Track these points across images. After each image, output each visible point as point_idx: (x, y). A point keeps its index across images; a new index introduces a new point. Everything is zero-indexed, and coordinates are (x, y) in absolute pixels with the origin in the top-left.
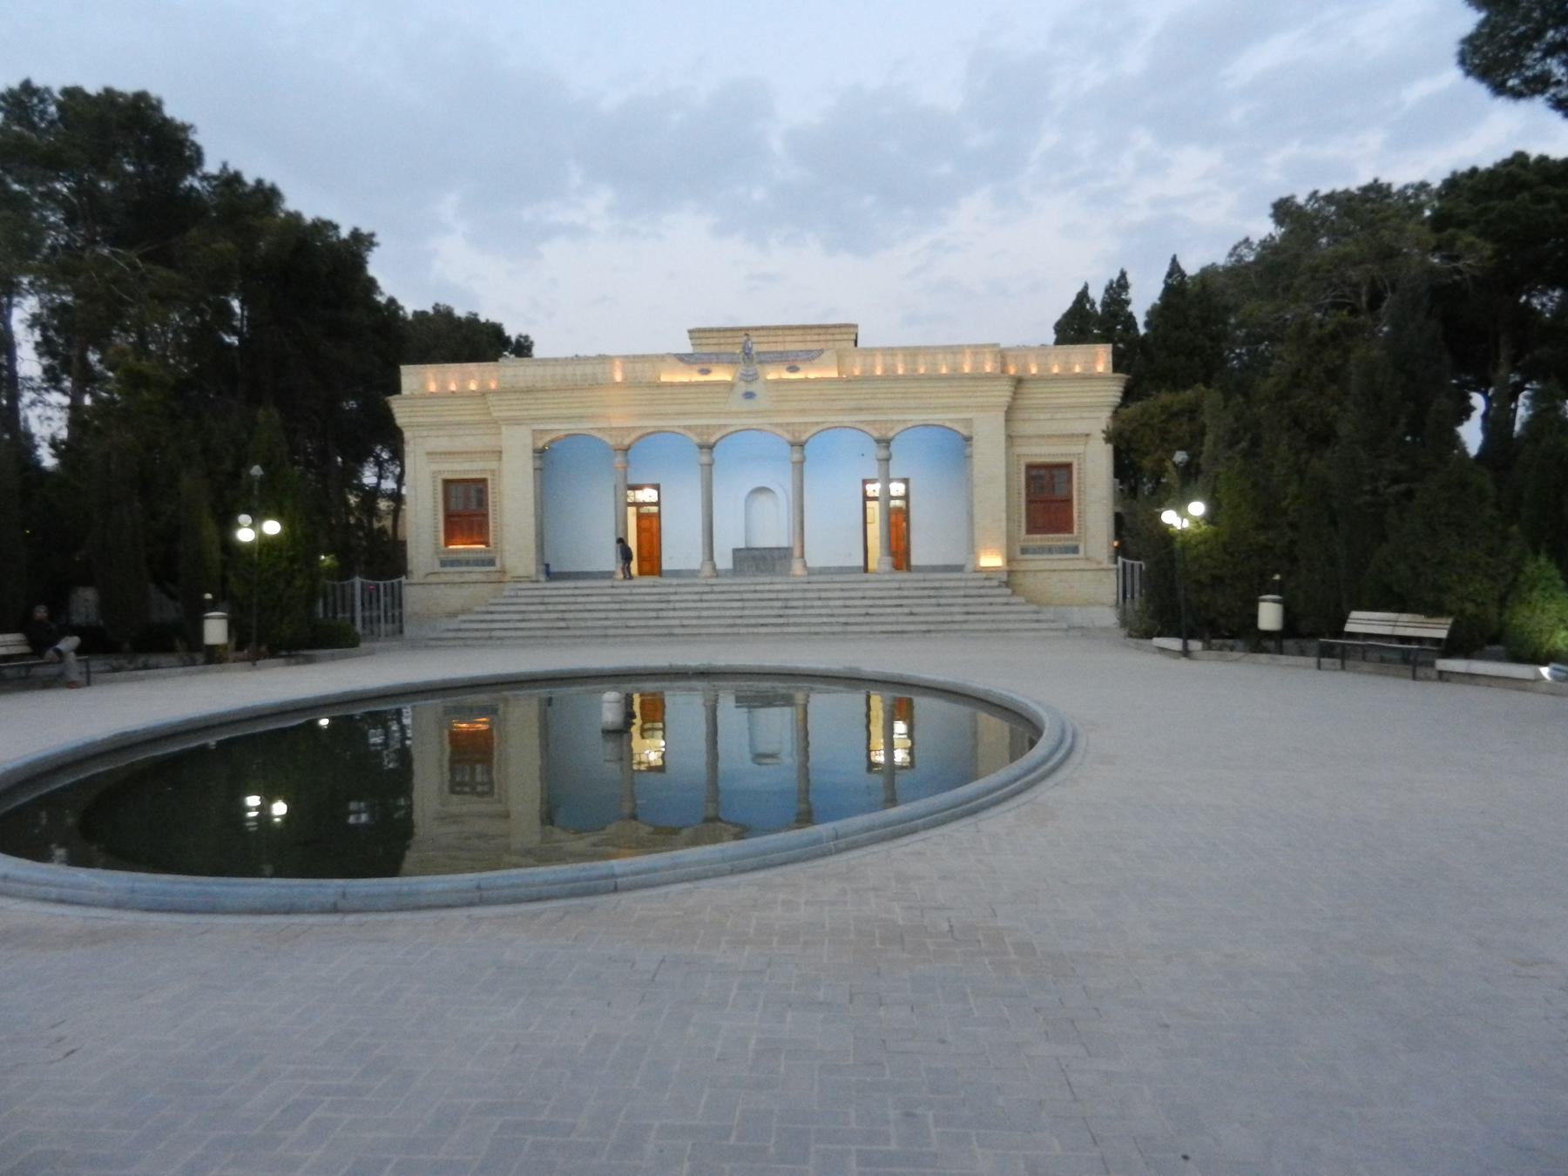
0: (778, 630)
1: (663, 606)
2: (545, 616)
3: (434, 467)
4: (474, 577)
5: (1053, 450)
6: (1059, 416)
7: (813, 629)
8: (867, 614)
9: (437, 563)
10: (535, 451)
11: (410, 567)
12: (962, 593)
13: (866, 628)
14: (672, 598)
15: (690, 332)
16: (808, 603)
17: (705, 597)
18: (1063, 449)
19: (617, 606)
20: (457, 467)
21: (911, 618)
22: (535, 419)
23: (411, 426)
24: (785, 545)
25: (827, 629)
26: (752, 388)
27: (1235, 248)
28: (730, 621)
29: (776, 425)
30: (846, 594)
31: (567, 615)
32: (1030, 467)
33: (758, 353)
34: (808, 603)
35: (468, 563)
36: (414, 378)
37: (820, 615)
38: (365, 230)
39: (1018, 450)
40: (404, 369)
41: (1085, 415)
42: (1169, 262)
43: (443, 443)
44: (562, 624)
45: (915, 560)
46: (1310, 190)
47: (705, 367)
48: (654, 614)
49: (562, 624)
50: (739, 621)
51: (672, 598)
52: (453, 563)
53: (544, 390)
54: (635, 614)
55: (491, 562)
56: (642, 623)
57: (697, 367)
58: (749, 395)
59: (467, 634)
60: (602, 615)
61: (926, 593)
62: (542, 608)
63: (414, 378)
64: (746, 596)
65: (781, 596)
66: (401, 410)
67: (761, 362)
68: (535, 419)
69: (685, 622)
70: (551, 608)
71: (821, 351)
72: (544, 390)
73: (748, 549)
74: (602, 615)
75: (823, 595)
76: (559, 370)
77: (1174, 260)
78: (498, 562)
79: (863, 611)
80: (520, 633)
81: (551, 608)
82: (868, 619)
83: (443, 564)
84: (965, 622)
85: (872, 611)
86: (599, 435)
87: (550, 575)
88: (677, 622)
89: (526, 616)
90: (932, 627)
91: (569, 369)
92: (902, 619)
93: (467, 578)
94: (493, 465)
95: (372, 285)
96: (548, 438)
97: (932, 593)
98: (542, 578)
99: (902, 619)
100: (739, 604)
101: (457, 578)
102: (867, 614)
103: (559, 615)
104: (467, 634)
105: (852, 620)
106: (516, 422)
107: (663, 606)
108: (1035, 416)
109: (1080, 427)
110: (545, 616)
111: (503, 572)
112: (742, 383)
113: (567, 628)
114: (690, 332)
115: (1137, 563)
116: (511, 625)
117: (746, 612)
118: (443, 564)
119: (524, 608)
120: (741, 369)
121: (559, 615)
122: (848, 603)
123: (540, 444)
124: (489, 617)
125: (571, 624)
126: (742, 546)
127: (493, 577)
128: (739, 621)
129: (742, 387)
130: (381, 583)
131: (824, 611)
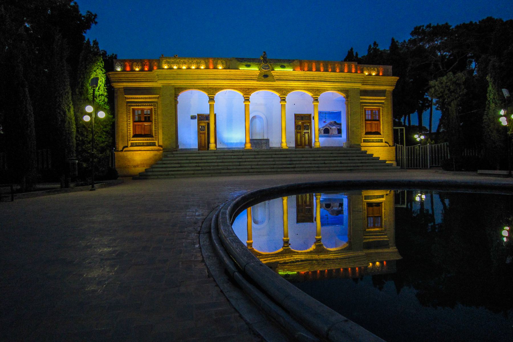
0: (293, 170)
7: (307, 169)
14: (243, 157)
19: (221, 160)
21: (342, 165)
24: (265, 138)
28: (272, 166)
31: (200, 165)
37: (307, 164)
46: (428, 24)
47: (249, 63)
51: (243, 157)
54: (231, 164)
56: (235, 167)
59: (157, 173)
60: (216, 164)
62: (188, 161)
64: (273, 156)
69: (253, 167)
70: (191, 161)
74: (216, 164)
75: (304, 156)
80: (182, 172)
81: (191, 161)
84: (362, 166)
88: (250, 167)
89: (182, 165)
90: (352, 168)
100: (272, 159)
103: (197, 165)
104: (157, 173)
105: (320, 165)
107: (241, 160)
110: (190, 165)
116: (177, 169)
117: (277, 163)
121: (197, 165)
122: (316, 159)
124: (164, 166)
131: (308, 162)
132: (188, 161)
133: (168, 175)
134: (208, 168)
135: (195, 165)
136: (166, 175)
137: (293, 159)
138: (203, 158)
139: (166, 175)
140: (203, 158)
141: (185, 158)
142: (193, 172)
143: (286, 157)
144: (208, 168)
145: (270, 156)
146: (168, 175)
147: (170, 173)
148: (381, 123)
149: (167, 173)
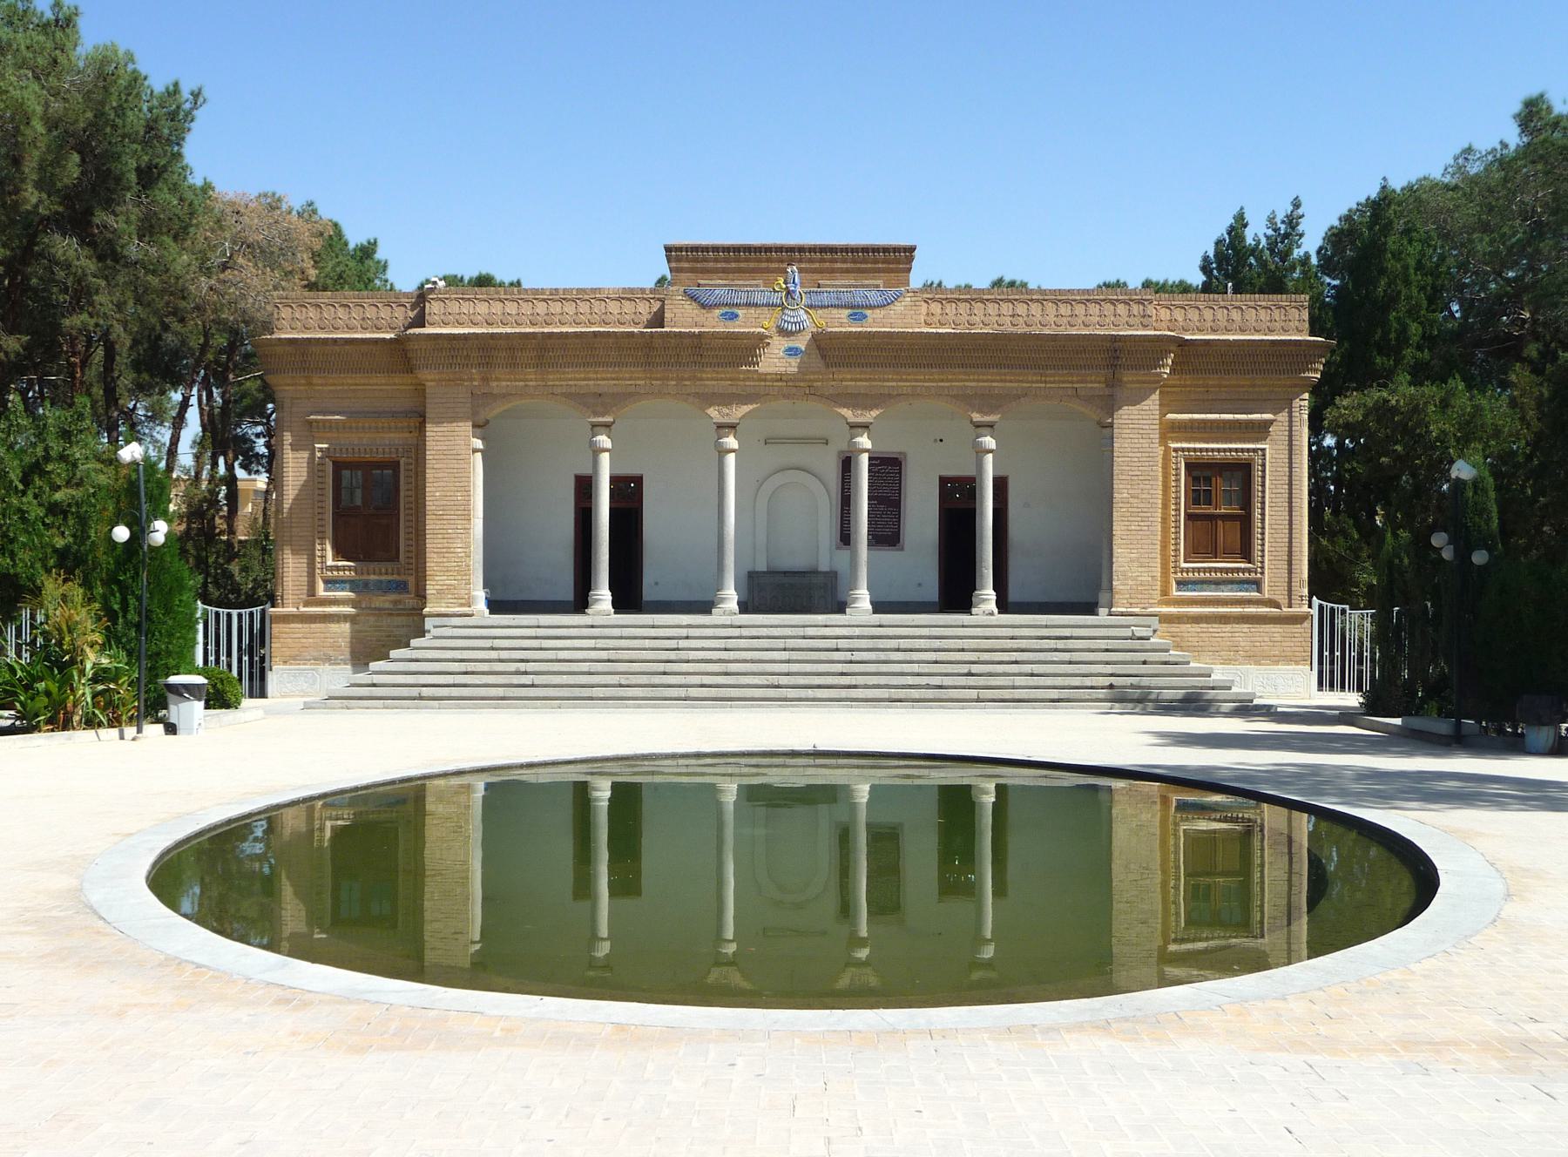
0: (844, 693)
1: (672, 655)
8: (970, 674)
9: (320, 586)
12: (1103, 644)
13: (973, 693)
14: (683, 643)
15: (668, 249)
16: (882, 656)
17: (731, 643)
19: (604, 655)
25: (915, 694)
30: (937, 644)
34: (882, 656)
45: (1013, 595)
48: (661, 667)
49: (526, 680)
50: (784, 680)
51: (683, 643)
55: (401, 587)
56: (644, 679)
57: (717, 312)
60: (585, 667)
61: (1052, 644)
62: (494, 655)
64: (791, 643)
65: (842, 643)
67: (811, 307)
70: (504, 655)
73: (771, 573)
74: (585, 667)
75: (904, 643)
78: (411, 586)
79: (965, 669)
81: (504, 655)
82: (971, 681)
85: (975, 668)
87: (495, 606)
89: (471, 667)
92: (1019, 681)
97: (1060, 644)
99: (1019, 681)
103: (522, 667)
105: (947, 681)
107: (672, 655)
111: (422, 596)
113: (533, 686)
114: (668, 249)
126: (762, 566)
128: (784, 680)
130: (235, 612)
135: (513, 667)
137: (858, 656)
141: (488, 643)
142: (500, 692)
143: (837, 650)
145: (780, 643)
147: (426, 691)
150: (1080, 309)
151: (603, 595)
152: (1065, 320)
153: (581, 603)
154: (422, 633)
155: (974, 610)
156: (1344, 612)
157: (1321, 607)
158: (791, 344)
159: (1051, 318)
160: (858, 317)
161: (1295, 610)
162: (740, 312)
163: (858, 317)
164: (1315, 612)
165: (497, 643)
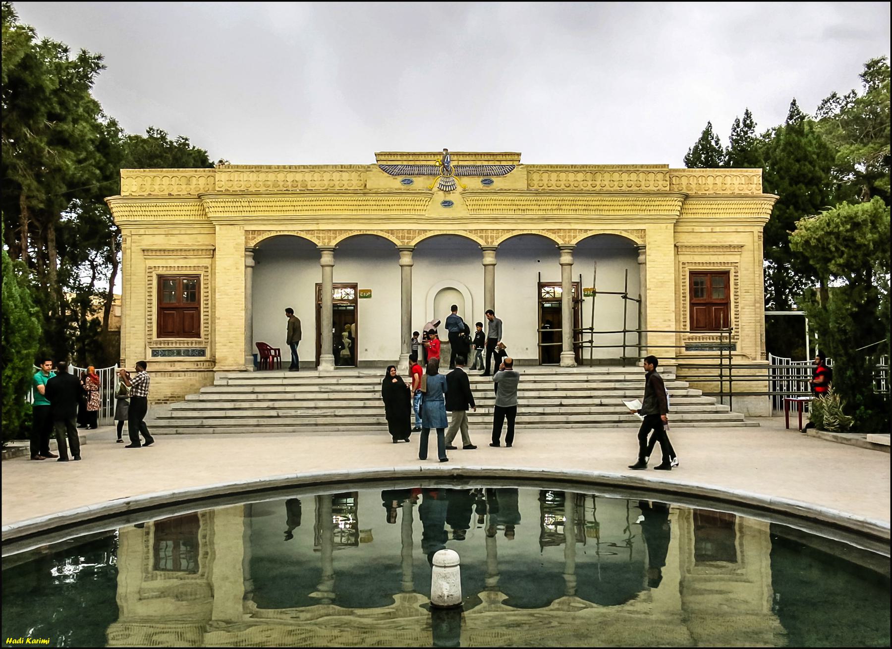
2: (256, 405)
3: (151, 263)
4: (184, 366)
5: (714, 259)
6: (718, 229)
9: (149, 352)
10: (246, 250)
11: (122, 357)
18: (722, 259)
19: (325, 396)
20: (171, 263)
22: (247, 220)
23: (129, 224)
26: (449, 198)
27: (825, 102)
29: (471, 231)
32: (692, 273)
33: (455, 167)
35: (179, 353)
36: (132, 180)
38: (92, 54)
39: (683, 259)
40: (123, 172)
41: (741, 229)
42: (788, 107)
43: (159, 241)
44: (273, 413)
47: (408, 177)
48: (361, 404)
49: (273, 413)
52: (164, 353)
53: (258, 194)
55: (202, 353)
57: (400, 178)
58: (447, 204)
60: (311, 404)
62: (253, 397)
63: (132, 180)
66: (119, 209)
67: (457, 175)
68: (247, 220)
71: (513, 167)
72: (258, 194)
74: (312, 404)
76: (271, 177)
77: (794, 103)
81: (261, 397)
83: (155, 353)
86: (308, 237)
89: (238, 405)
91: (281, 177)
93: (178, 367)
94: (206, 262)
95: (94, 108)
96: (260, 238)
98: (251, 367)
101: (168, 367)
102: (561, 405)
103: (270, 404)
106: (231, 223)
108: (697, 229)
109: (735, 239)
110: (256, 405)
111: (213, 362)
112: (441, 192)
113: (278, 417)
115: (784, 359)
118: (155, 353)
119: (235, 397)
120: (439, 180)
121: (270, 404)
123: (252, 244)
125: (281, 413)
127: (202, 367)
129: (440, 197)
132: (253, 397)
133: (202, 426)
134: (293, 412)
136: (198, 427)
138: (288, 389)
139: (198, 427)
140: (288, 389)
144: (293, 412)
146: (202, 426)
148: (733, 305)
149: (198, 422)
150: (625, 176)
151: (328, 358)
152: (616, 183)
153: (318, 363)
154: (213, 385)
155: (562, 364)
156: (788, 362)
157: (774, 360)
158: (447, 199)
159: (607, 183)
160: (488, 182)
161: (759, 361)
162: (414, 179)
163: (488, 182)
164: (770, 362)
165: (257, 389)
